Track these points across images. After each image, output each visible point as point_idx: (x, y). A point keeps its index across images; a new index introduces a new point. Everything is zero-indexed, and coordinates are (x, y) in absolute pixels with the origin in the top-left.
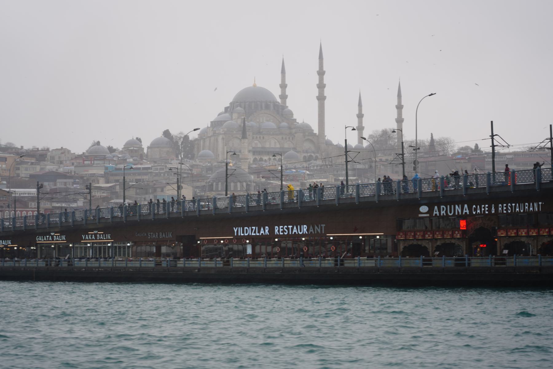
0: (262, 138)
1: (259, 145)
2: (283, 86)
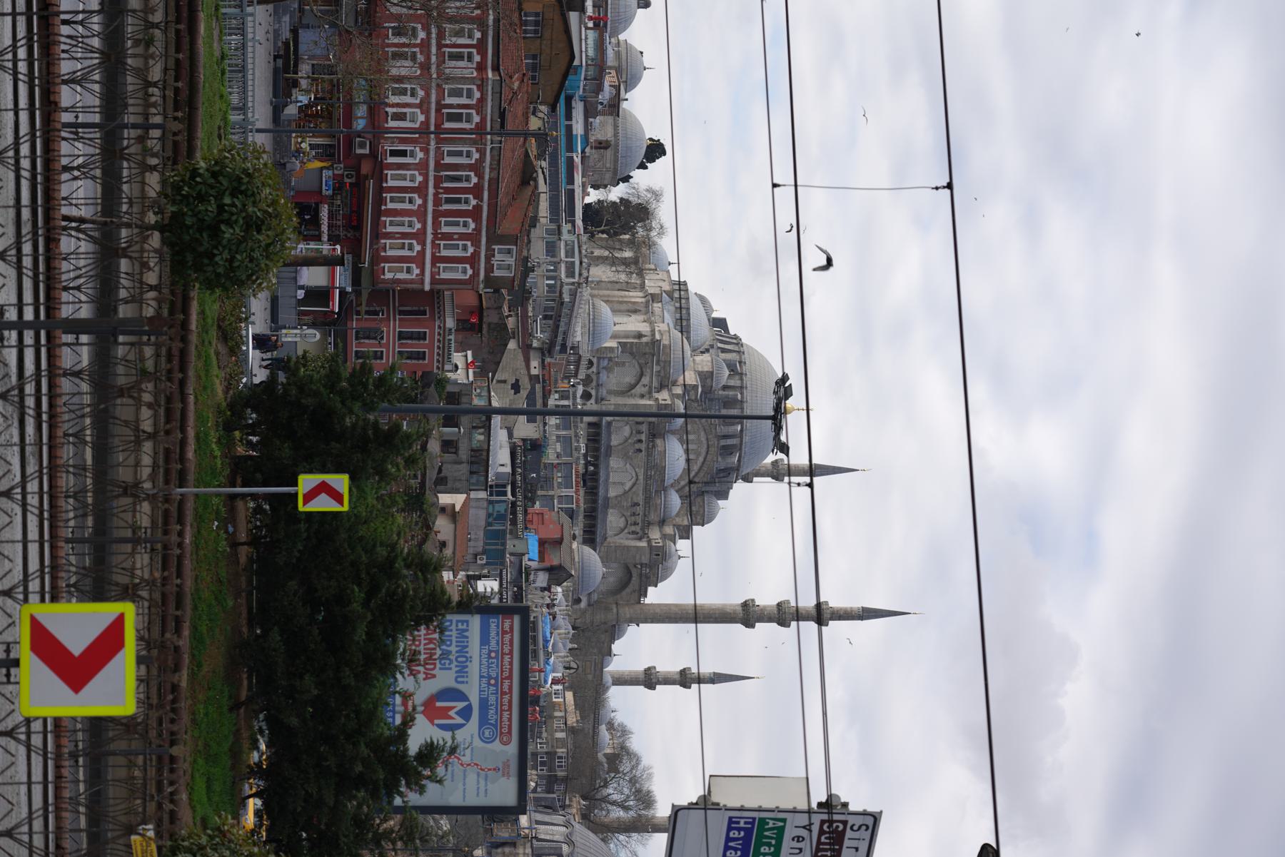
0: (637, 446)
1: (615, 441)
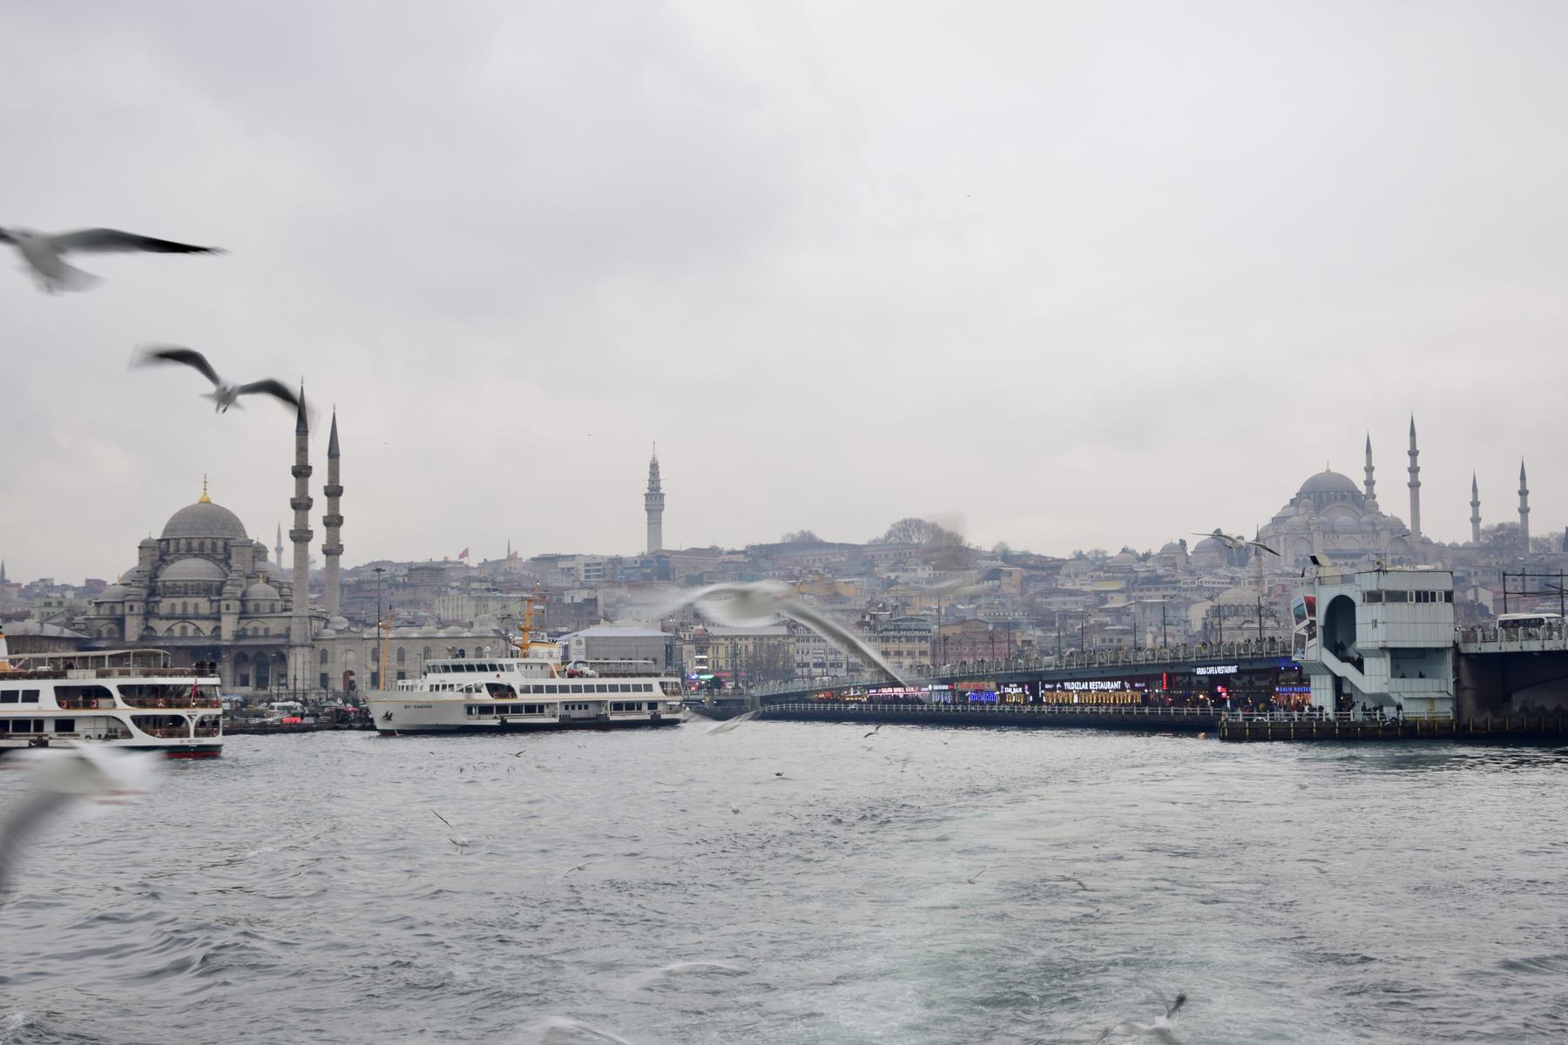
1: (1333, 547)
2: (1369, 469)
